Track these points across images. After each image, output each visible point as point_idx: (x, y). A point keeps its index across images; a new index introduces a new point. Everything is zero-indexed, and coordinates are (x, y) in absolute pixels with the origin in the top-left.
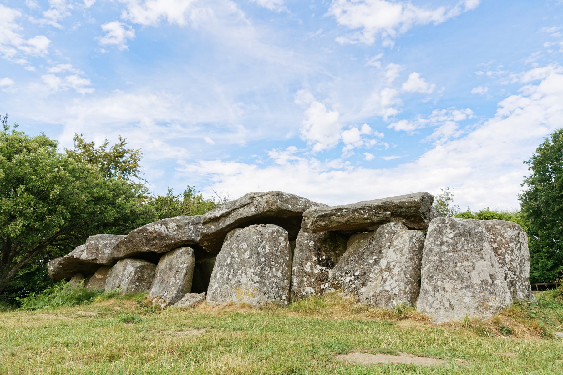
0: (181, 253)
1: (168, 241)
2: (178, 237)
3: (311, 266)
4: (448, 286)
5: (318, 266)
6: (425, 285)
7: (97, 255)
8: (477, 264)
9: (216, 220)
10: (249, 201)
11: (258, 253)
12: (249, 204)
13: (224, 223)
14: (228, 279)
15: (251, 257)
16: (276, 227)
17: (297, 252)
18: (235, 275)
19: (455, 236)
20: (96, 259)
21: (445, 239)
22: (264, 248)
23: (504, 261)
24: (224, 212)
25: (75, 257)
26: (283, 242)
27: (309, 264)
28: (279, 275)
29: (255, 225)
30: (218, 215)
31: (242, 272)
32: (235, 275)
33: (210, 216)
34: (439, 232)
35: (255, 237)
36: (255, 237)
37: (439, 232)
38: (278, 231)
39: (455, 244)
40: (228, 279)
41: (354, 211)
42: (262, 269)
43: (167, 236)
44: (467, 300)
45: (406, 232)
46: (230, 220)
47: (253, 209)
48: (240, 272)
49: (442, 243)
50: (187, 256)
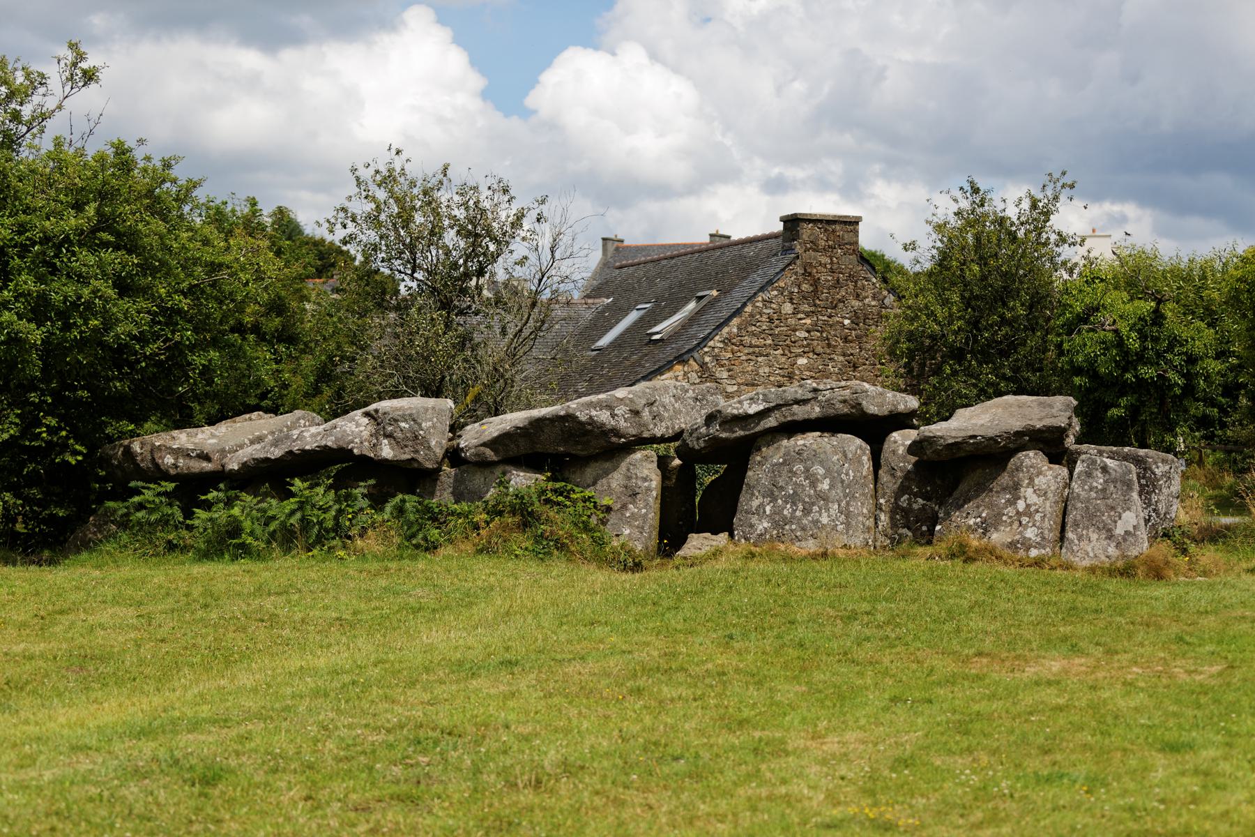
0: (641, 460)
1: (614, 439)
2: (633, 431)
3: (909, 499)
4: (1094, 536)
5: (920, 501)
6: (1070, 535)
7: (417, 452)
8: (1124, 515)
9: (743, 419)
10: (810, 395)
11: (842, 482)
12: (808, 400)
13: (758, 424)
14: (793, 517)
15: (832, 486)
16: (858, 441)
17: (884, 476)
18: (807, 511)
19: (1105, 482)
20: (413, 459)
21: (1095, 484)
22: (847, 474)
23: (1150, 500)
24: (761, 407)
25: (355, 451)
26: (867, 464)
27: (906, 497)
28: (865, 511)
29: (818, 433)
30: (751, 411)
31: (820, 509)
32: (807, 511)
33: (735, 412)
34: (1089, 475)
35: (835, 458)
36: (835, 458)
37: (1089, 475)
38: (861, 447)
39: (1104, 490)
40: (793, 517)
41: (991, 438)
42: (848, 504)
43: (615, 432)
44: (1110, 549)
45: (1050, 469)
46: (771, 422)
47: (817, 409)
48: (816, 508)
49: (1091, 489)
50: (650, 466)
